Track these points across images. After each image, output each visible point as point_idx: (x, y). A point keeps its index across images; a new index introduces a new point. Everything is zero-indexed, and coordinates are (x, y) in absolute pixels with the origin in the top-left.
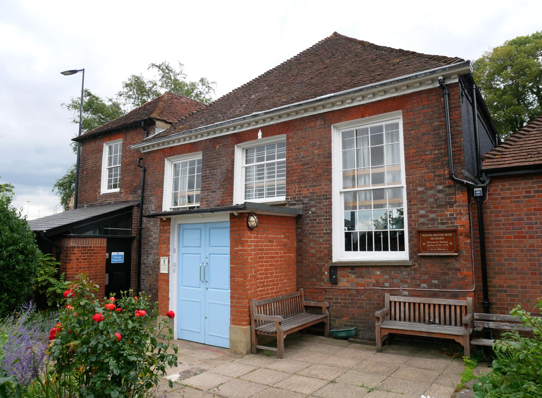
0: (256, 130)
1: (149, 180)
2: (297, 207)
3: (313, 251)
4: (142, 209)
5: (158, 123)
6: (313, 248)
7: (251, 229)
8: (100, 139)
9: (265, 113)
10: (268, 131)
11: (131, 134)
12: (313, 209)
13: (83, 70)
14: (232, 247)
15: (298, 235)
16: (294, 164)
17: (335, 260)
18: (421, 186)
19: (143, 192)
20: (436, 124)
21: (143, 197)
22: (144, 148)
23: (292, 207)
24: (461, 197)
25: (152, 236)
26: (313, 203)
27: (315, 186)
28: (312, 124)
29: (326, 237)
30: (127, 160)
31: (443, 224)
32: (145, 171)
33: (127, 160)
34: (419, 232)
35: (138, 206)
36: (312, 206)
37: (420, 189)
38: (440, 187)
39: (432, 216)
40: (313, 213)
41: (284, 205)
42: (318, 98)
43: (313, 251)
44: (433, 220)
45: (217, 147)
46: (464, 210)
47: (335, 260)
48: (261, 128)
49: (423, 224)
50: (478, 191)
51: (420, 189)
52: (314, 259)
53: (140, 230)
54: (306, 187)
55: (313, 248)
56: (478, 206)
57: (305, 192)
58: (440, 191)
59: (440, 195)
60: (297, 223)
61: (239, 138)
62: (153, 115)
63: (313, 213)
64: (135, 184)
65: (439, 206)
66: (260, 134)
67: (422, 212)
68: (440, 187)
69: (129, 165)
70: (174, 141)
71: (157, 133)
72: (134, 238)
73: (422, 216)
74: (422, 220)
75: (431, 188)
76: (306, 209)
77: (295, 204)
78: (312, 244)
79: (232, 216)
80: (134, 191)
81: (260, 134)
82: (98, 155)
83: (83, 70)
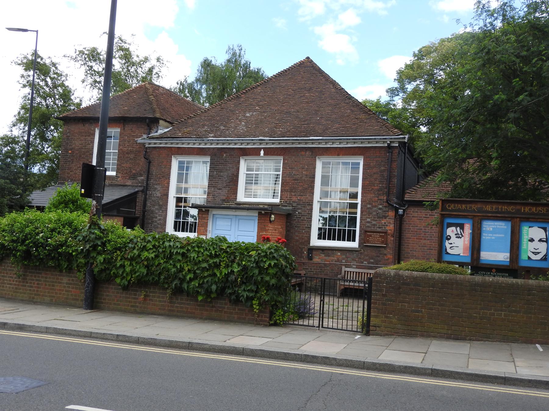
0: (260, 149)
1: (154, 170)
2: (288, 208)
3: (297, 238)
4: (146, 194)
5: (161, 122)
6: (297, 236)
7: (270, 221)
8: (91, 123)
9: (270, 140)
10: (269, 152)
11: (129, 127)
12: (299, 211)
13: (37, 31)
14: (258, 233)
15: (287, 226)
16: (287, 179)
17: (311, 245)
18: (370, 204)
19: (148, 179)
20: (383, 168)
21: (147, 184)
22: (150, 144)
23: (284, 208)
24: (391, 214)
25: (156, 218)
26: (299, 206)
27: (302, 196)
28: (303, 153)
29: (307, 230)
30: (125, 149)
31: (379, 228)
32: (150, 162)
33: (125, 149)
34: (366, 231)
35: (142, 191)
36: (299, 209)
37: (369, 206)
38: (381, 206)
39: (374, 222)
40: (299, 213)
41: (279, 205)
42: (311, 138)
43: (297, 238)
44: (374, 225)
45: (225, 155)
46: (392, 221)
47: (311, 245)
48: (264, 149)
49: (369, 227)
50: (401, 211)
51: (369, 206)
52: (298, 243)
53: (144, 211)
54: (295, 195)
55: (297, 236)
56: (400, 220)
57: (294, 199)
58: (380, 209)
59: (380, 211)
60: (287, 219)
61: (245, 152)
62: (158, 115)
63: (299, 213)
64: (134, 172)
65: (379, 217)
66: (262, 153)
67: (369, 220)
68: (381, 206)
69: (128, 153)
70: (183, 144)
71: (160, 132)
72: (138, 218)
73: (368, 222)
74: (368, 224)
75: (375, 206)
76: (295, 210)
77: (287, 206)
78: (297, 234)
79: (260, 214)
80: (134, 177)
81: (262, 153)
82: (89, 138)
83: (37, 31)
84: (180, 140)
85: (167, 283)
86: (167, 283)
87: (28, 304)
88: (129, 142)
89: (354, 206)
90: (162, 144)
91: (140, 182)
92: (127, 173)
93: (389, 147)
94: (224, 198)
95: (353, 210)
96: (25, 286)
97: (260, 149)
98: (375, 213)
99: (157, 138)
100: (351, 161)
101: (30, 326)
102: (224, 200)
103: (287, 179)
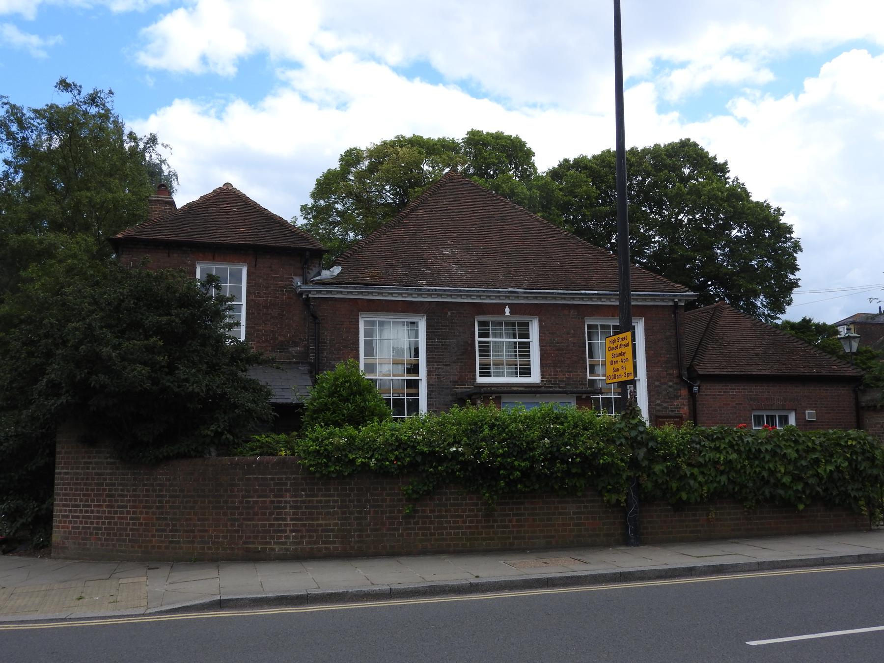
0: (504, 305)
18: (658, 381)
20: (668, 334)
24: (684, 392)
28: (566, 312)
31: (672, 411)
34: (658, 417)
37: (657, 383)
38: (671, 383)
39: (665, 405)
42: (583, 292)
44: (666, 408)
45: (449, 313)
46: (686, 402)
48: (510, 305)
49: (659, 411)
50: (696, 389)
51: (657, 383)
54: (561, 371)
57: (561, 376)
58: (670, 387)
59: (671, 389)
65: (670, 398)
67: (658, 402)
68: (671, 383)
73: (658, 405)
74: (658, 408)
75: (665, 384)
84: (355, 288)
85: (804, 492)
86: (804, 492)
87: (484, 555)
88: (267, 288)
89: (413, 385)
90: (338, 293)
91: (294, 357)
92: (267, 341)
93: (676, 306)
94: (456, 378)
95: (412, 391)
96: (492, 527)
97: (504, 305)
98: (664, 393)
99: (332, 283)
100: (611, 324)
101: (732, 566)
102: (455, 382)
103: (548, 348)
